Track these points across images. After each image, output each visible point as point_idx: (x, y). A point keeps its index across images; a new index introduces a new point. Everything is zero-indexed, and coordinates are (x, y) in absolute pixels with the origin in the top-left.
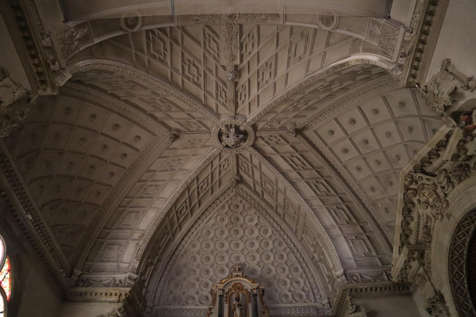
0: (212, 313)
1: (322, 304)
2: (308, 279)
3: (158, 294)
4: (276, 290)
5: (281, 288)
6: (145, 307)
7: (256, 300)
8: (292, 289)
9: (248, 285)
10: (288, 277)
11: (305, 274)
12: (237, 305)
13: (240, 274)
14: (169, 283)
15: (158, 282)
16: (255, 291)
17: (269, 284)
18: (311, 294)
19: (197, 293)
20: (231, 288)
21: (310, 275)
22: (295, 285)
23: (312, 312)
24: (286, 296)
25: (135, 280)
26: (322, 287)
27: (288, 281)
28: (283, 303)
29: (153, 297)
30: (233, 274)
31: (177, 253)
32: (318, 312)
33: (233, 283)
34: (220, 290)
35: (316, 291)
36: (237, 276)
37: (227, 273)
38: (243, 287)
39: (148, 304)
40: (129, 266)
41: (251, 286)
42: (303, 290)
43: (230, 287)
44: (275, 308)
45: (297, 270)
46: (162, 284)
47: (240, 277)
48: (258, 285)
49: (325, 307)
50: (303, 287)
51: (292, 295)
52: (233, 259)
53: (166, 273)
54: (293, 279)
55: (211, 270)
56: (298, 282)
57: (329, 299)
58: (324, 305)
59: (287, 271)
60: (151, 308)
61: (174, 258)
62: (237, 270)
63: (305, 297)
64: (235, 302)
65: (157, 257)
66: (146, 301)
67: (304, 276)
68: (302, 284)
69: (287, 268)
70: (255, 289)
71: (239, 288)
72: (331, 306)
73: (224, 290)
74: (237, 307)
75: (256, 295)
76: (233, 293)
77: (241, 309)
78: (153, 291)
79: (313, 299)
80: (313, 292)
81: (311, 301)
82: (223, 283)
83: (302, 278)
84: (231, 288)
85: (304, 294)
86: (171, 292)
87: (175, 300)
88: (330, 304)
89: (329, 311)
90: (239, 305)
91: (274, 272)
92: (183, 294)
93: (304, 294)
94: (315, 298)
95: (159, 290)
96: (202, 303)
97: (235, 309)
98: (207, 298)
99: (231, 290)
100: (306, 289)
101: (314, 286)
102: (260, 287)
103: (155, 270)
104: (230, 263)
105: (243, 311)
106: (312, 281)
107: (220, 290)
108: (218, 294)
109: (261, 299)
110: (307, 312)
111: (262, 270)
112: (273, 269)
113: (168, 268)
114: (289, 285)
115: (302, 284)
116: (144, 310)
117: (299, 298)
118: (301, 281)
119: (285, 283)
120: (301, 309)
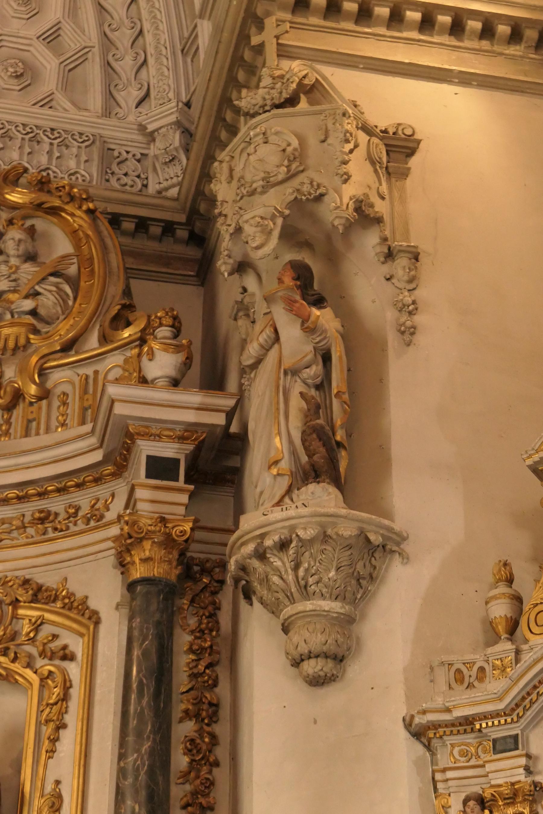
1: (142, 128)
18: (94, 71)
23: (72, 164)
26: (164, 37)
32: (106, 171)
35: (126, 66)
42: (52, 38)
49: (159, 146)
58: (151, 137)
63: (50, 82)
79: (95, 100)
85: (48, 64)
89: (175, 170)
94: (109, 96)
100: (71, 41)
101: (123, 37)
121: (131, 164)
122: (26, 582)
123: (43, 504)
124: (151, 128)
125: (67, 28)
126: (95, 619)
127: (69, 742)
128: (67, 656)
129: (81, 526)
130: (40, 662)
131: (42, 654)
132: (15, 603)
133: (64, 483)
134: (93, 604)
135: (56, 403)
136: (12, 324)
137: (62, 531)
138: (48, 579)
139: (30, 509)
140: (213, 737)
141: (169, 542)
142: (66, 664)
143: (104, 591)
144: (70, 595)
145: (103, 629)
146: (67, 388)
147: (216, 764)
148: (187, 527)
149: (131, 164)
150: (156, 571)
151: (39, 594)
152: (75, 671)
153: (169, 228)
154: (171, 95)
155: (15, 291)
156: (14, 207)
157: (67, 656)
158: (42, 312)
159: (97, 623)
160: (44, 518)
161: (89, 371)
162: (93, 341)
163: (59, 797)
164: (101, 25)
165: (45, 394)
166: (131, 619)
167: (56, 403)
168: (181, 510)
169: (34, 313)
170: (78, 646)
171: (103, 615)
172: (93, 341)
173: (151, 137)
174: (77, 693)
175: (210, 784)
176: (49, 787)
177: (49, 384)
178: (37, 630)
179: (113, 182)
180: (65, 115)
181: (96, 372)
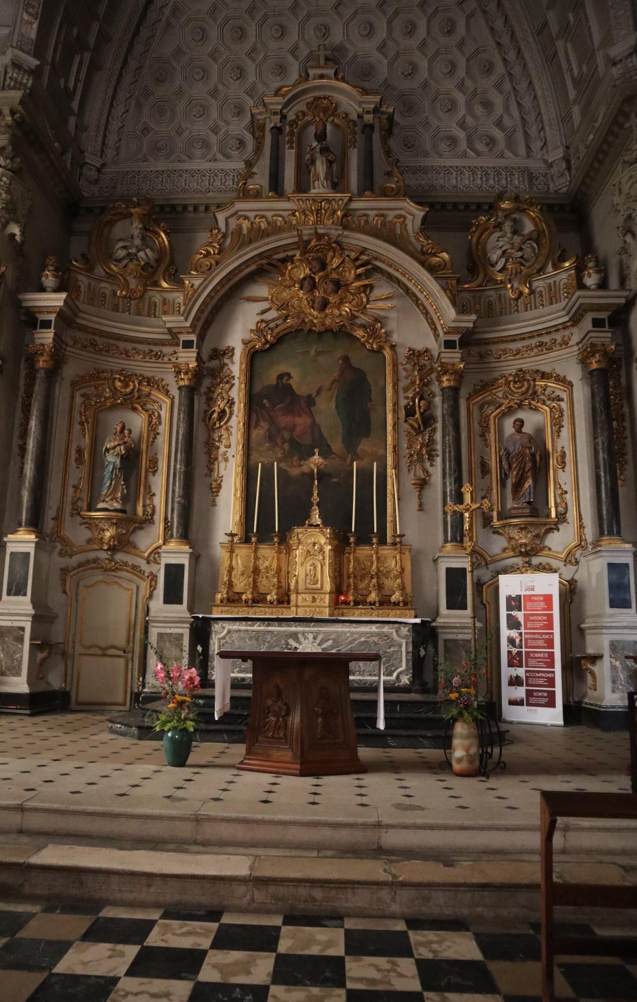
0: (254, 173)
1: (545, 161)
2: (516, 96)
3: (112, 138)
4: (426, 124)
5: (439, 118)
6: (81, 167)
7: (370, 139)
8: (469, 120)
9: (350, 101)
10: (461, 86)
11: (511, 80)
12: (318, 150)
13: (331, 72)
14: (139, 105)
15: (108, 102)
16: (368, 118)
17: (410, 108)
18: (520, 137)
19: (215, 130)
20: (305, 109)
21: (523, 86)
22: (479, 110)
23: (516, 182)
24: (453, 141)
25: (31, 72)
27: (461, 99)
28: (441, 156)
29: (100, 143)
30: (311, 72)
31: (152, 16)
32: (531, 183)
33: (309, 97)
34: (275, 113)
35: (533, 131)
36: (322, 77)
37: (294, 76)
38: (336, 108)
39: (92, 159)
40: (12, 33)
41: (360, 104)
42: (499, 124)
43: (300, 106)
44: (424, 170)
45: (488, 69)
46: (119, 110)
47: (329, 78)
48: (377, 99)
49: (554, 170)
50: (501, 117)
51: (469, 139)
52: (310, 33)
53: (127, 79)
54: (475, 93)
55: (250, 67)
56: (487, 105)
57: (568, 148)
58: (551, 165)
59: (461, 73)
60: (99, 170)
61: (145, 32)
62: (322, 62)
64: (315, 144)
65: (96, 26)
66: (82, 152)
67: (507, 86)
68: (499, 110)
69: (462, 63)
70: (368, 112)
71: (325, 110)
72: (569, 168)
73: (284, 117)
74: (318, 155)
75: (372, 127)
76: (308, 124)
77: (330, 163)
78: (98, 126)
79: (522, 151)
80: (525, 132)
81: (516, 155)
82: (283, 96)
83: (501, 92)
84: (305, 109)
85: (499, 135)
86: (146, 130)
87: (159, 149)
88: (568, 162)
89: (562, 180)
90: (325, 150)
91: (423, 74)
92: (179, 133)
93: (499, 135)
94: (528, 147)
95: (115, 126)
96: (228, 157)
97: (313, 162)
98: (242, 143)
99: (304, 114)
100: (507, 122)
101: (531, 117)
102: (383, 109)
103: (95, 67)
104: (302, 45)
105: (334, 166)
106: (527, 102)
107: (275, 113)
108: (269, 126)
109: (385, 140)
110: (504, 182)
111: (391, 64)
112: (424, 64)
113: (133, 64)
114: (462, 111)
115: (499, 110)
116: (81, 174)
117: (487, 145)
118: (498, 100)
119: (452, 107)
120: (487, 174)
121: (541, 178)
122: (538, 371)
123: (540, 339)
124: (550, 161)
125: (505, 117)
126: (570, 384)
127: (565, 433)
128: (562, 400)
129: (558, 347)
130: (548, 403)
131: (549, 399)
132: (534, 380)
133: (548, 331)
134: (568, 378)
135: (537, 296)
136: (513, 263)
137: (550, 349)
138: (546, 369)
139: (534, 342)
140: (624, 427)
141: (605, 354)
142: (559, 403)
143: (574, 373)
144: (558, 375)
145: (574, 388)
146: (542, 289)
147: (626, 438)
148: (613, 347)
149: (541, 178)
150: (603, 366)
151: (544, 376)
152: (564, 405)
153: (562, 207)
154: (559, 144)
155: (512, 248)
156: (504, 210)
157: (562, 400)
158: (526, 256)
159: (572, 386)
160: (541, 344)
161: (551, 281)
162: (550, 268)
163: (564, 453)
164: (520, 113)
165: (532, 292)
166: (592, 385)
167: (537, 296)
168: (609, 340)
169: (522, 257)
170: (564, 396)
171: (574, 383)
172: (550, 268)
173: (551, 165)
174: (566, 414)
175: (624, 445)
176: (559, 450)
177: (533, 288)
178: (545, 390)
179: (535, 189)
180: (511, 160)
181: (555, 282)
